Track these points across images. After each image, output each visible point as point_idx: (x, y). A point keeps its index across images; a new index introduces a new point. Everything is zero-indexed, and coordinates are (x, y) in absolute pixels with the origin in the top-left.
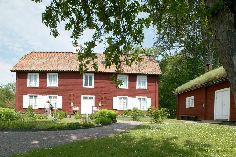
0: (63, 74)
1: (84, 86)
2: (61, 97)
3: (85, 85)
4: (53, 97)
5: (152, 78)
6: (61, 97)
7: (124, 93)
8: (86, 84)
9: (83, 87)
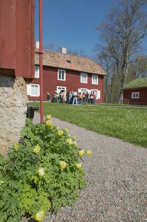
1: (58, 79)
3: (59, 78)
4: (34, 86)
5: (101, 77)
7: (83, 86)
8: (60, 78)
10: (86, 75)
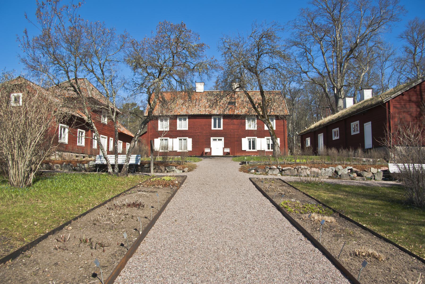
0: (191, 117)
1: (213, 128)
2: (191, 139)
3: (214, 127)
6: (191, 139)
8: (215, 126)
9: (212, 129)
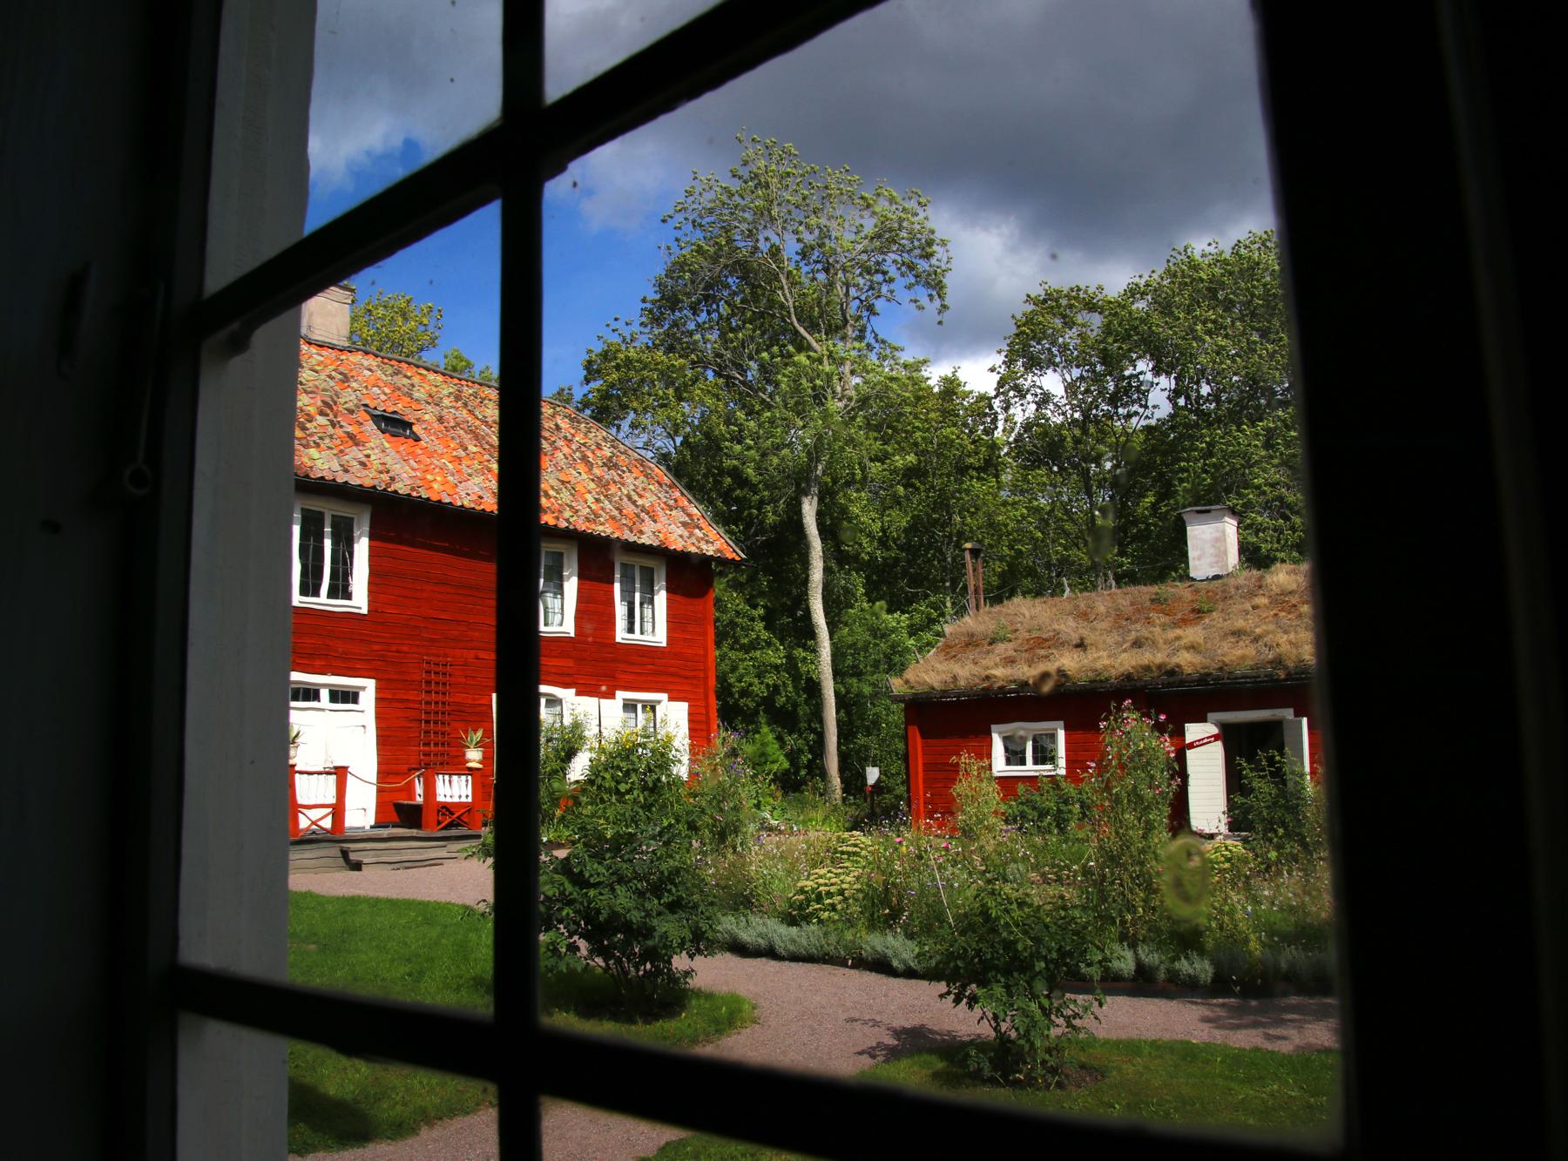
10: (652, 570)
